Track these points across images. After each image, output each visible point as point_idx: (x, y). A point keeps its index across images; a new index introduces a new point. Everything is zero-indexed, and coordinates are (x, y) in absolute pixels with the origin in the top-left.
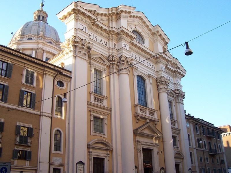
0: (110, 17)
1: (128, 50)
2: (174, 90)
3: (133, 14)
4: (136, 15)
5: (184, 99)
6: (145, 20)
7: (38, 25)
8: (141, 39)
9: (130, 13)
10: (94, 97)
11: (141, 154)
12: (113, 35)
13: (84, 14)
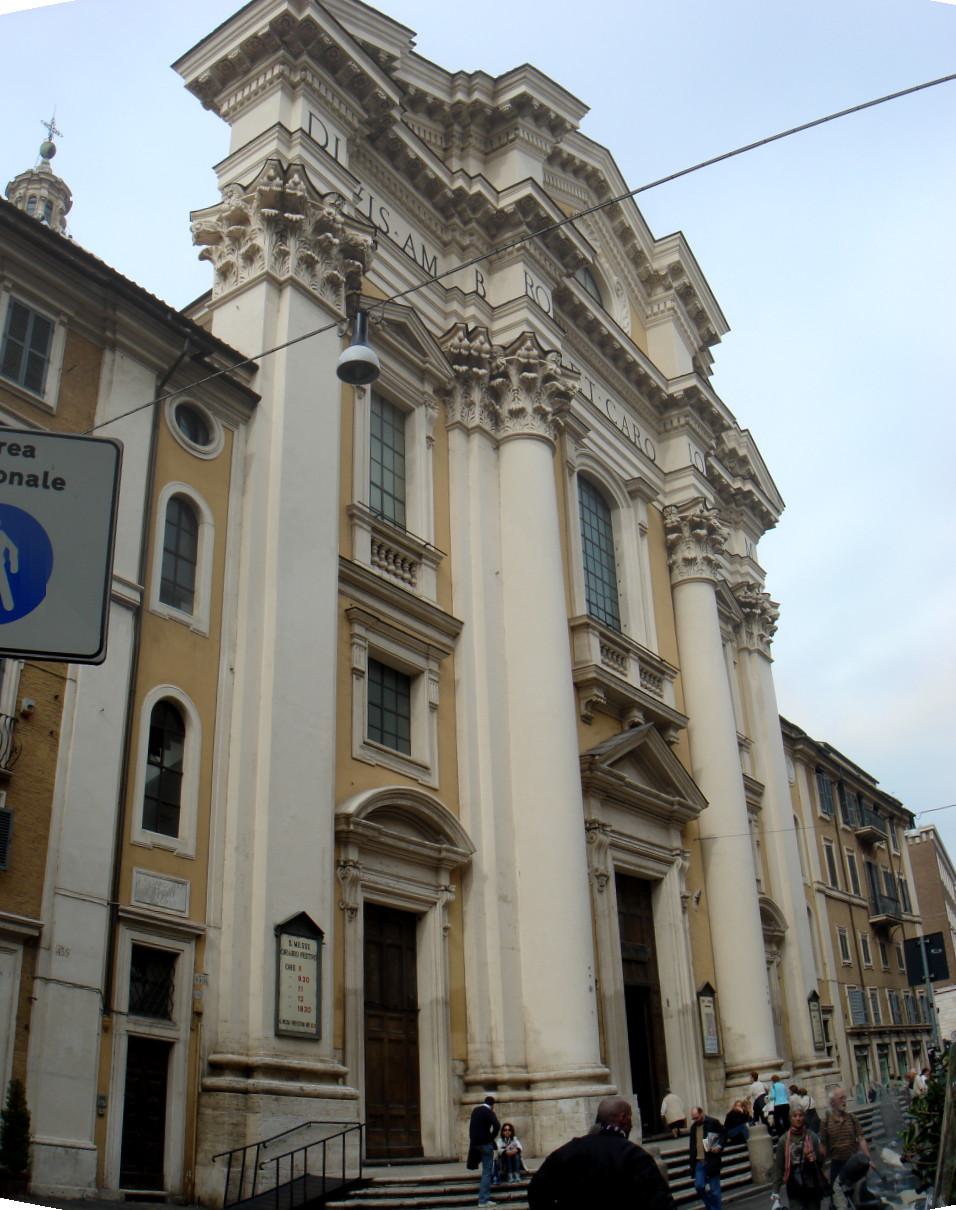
10: (373, 542)
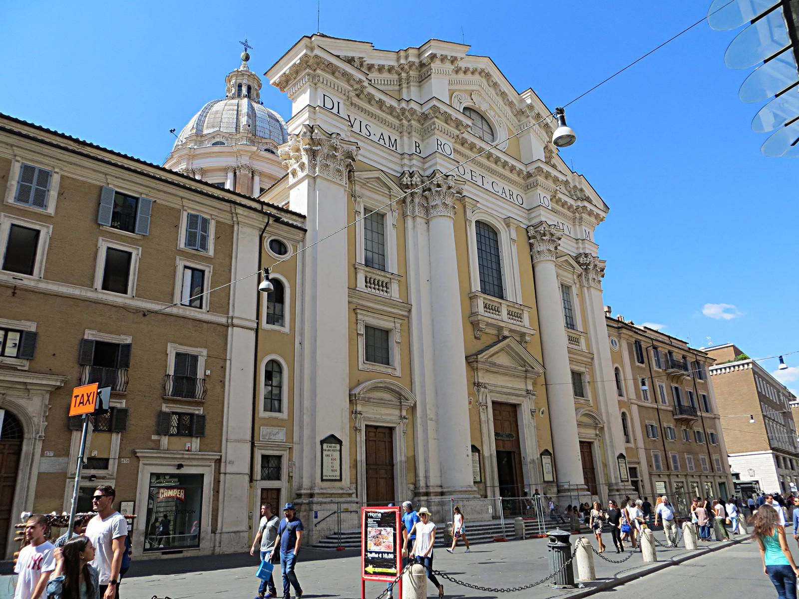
0: (404, 75)
1: (452, 156)
2: (575, 255)
3: (462, 65)
4: (471, 66)
5: (601, 279)
6: (497, 77)
7: (236, 108)
8: (486, 127)
9: (453, 60)
10: (366, 278)
12: (413, 122)
13: (332, 70)
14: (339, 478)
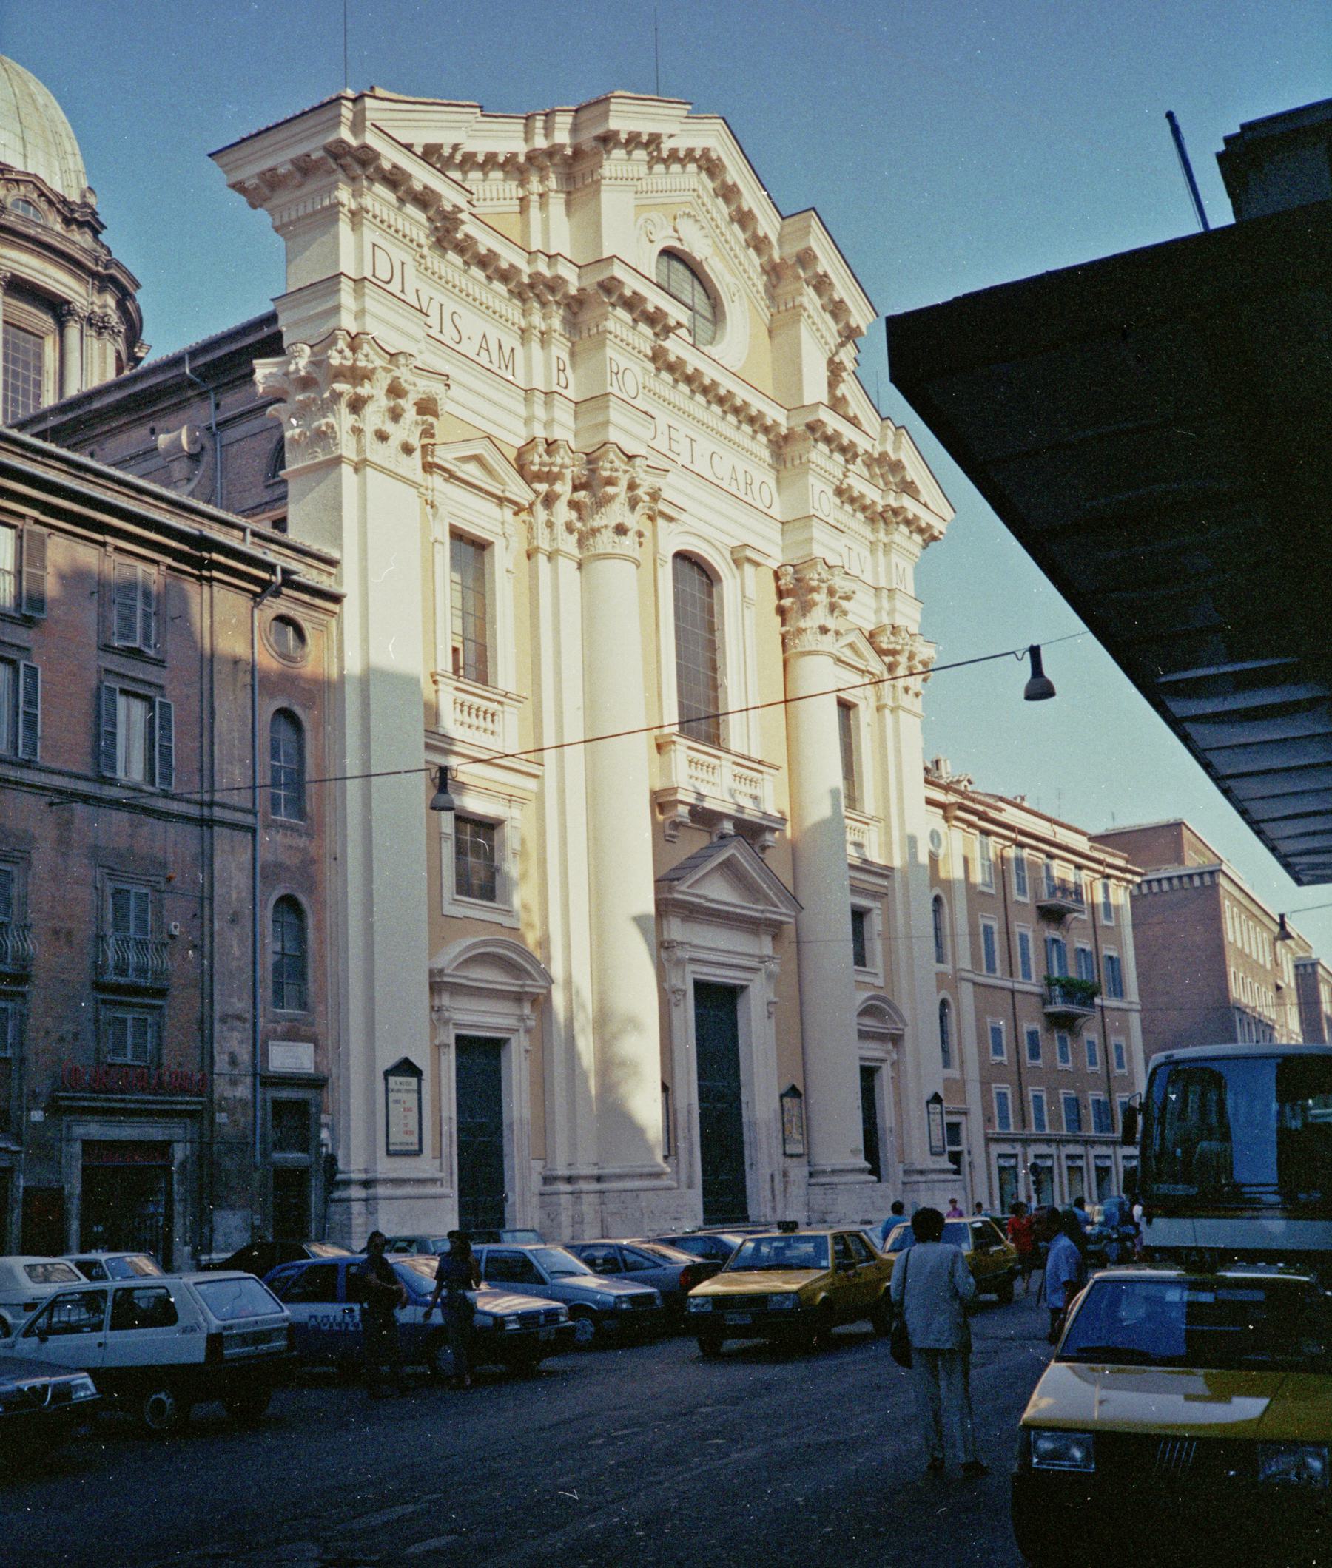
6: (736, 172)
11: (687, 1012)
14: (416, 1148)
